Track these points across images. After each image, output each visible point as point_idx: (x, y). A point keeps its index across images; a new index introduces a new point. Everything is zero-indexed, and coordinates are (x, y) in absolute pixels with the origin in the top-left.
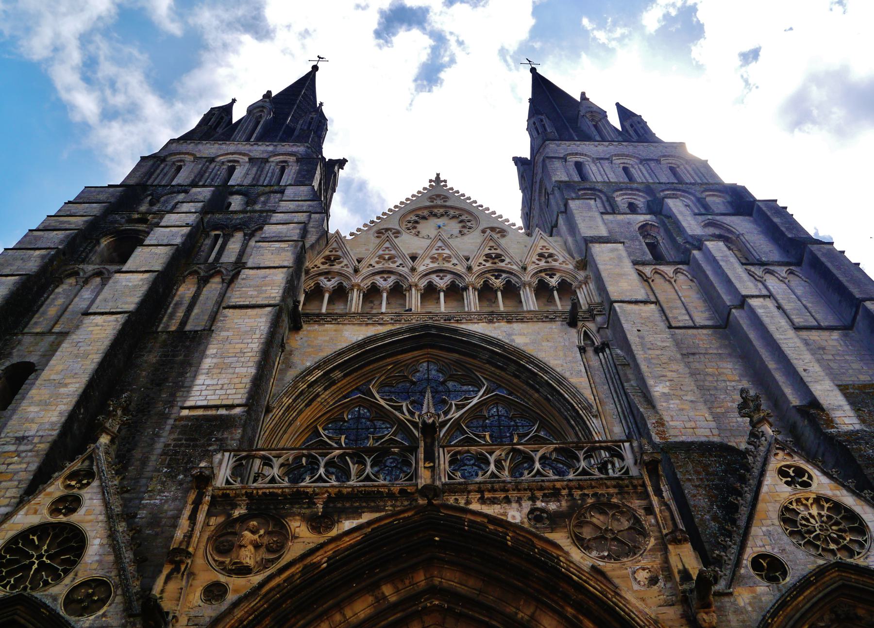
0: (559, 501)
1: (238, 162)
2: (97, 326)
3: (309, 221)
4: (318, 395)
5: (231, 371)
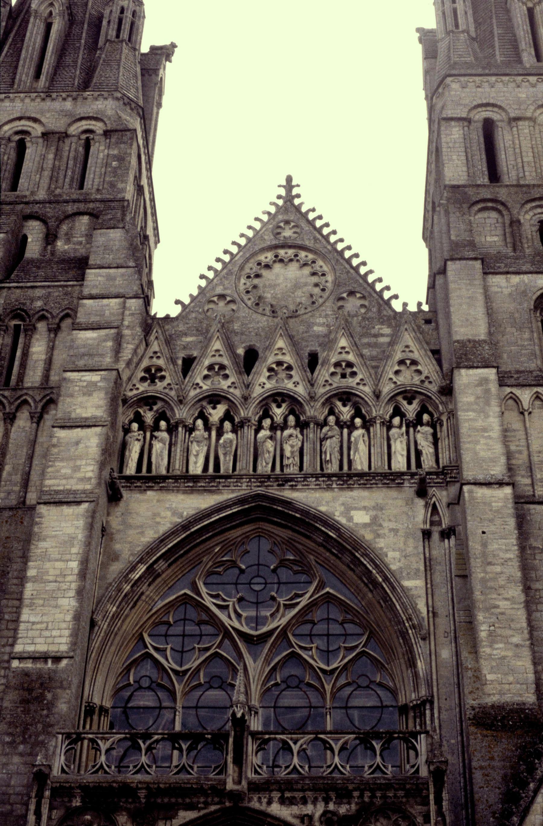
0: (349, 803)
1: (27, 133)
3: (123, 313)
4: (142, 594)
5: (53, 603)
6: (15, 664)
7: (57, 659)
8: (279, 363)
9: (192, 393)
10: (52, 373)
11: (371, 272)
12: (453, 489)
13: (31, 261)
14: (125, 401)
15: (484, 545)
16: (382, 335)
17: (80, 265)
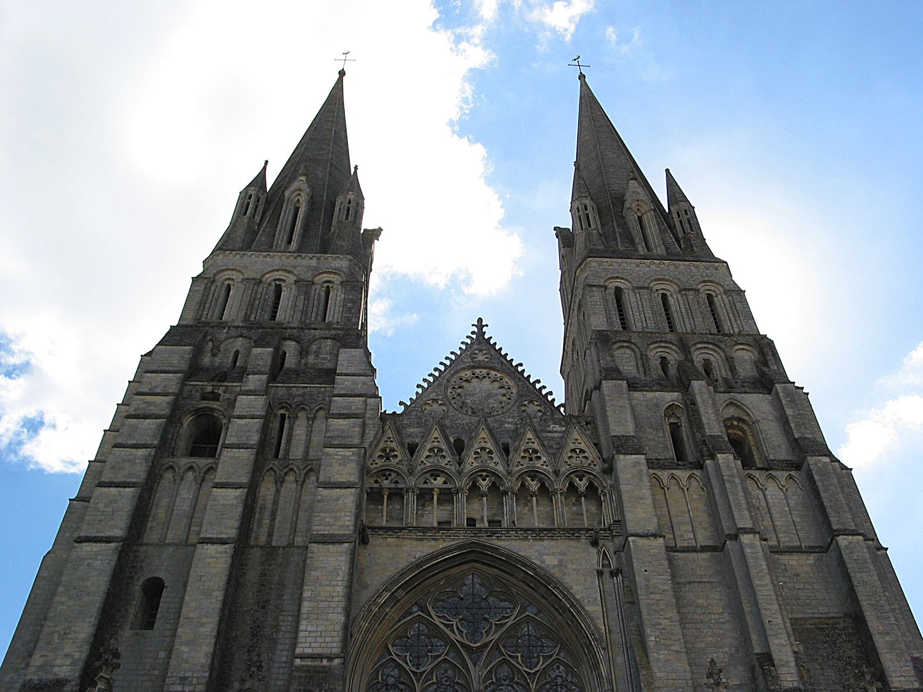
1: (284, 281)
2: (211, 557)
4: (386, 614)
5: (324, 617)
6: (298, 662)
7: (330, 658)
8: (483, 449)
9: (419, 468)
10: (311, 449)
11: (544, 387)
12: (619, 541)
13: (289, 369)
14: (368, 472)
15: (647, 579)
16: (556, 432)
17: (330, 375)
